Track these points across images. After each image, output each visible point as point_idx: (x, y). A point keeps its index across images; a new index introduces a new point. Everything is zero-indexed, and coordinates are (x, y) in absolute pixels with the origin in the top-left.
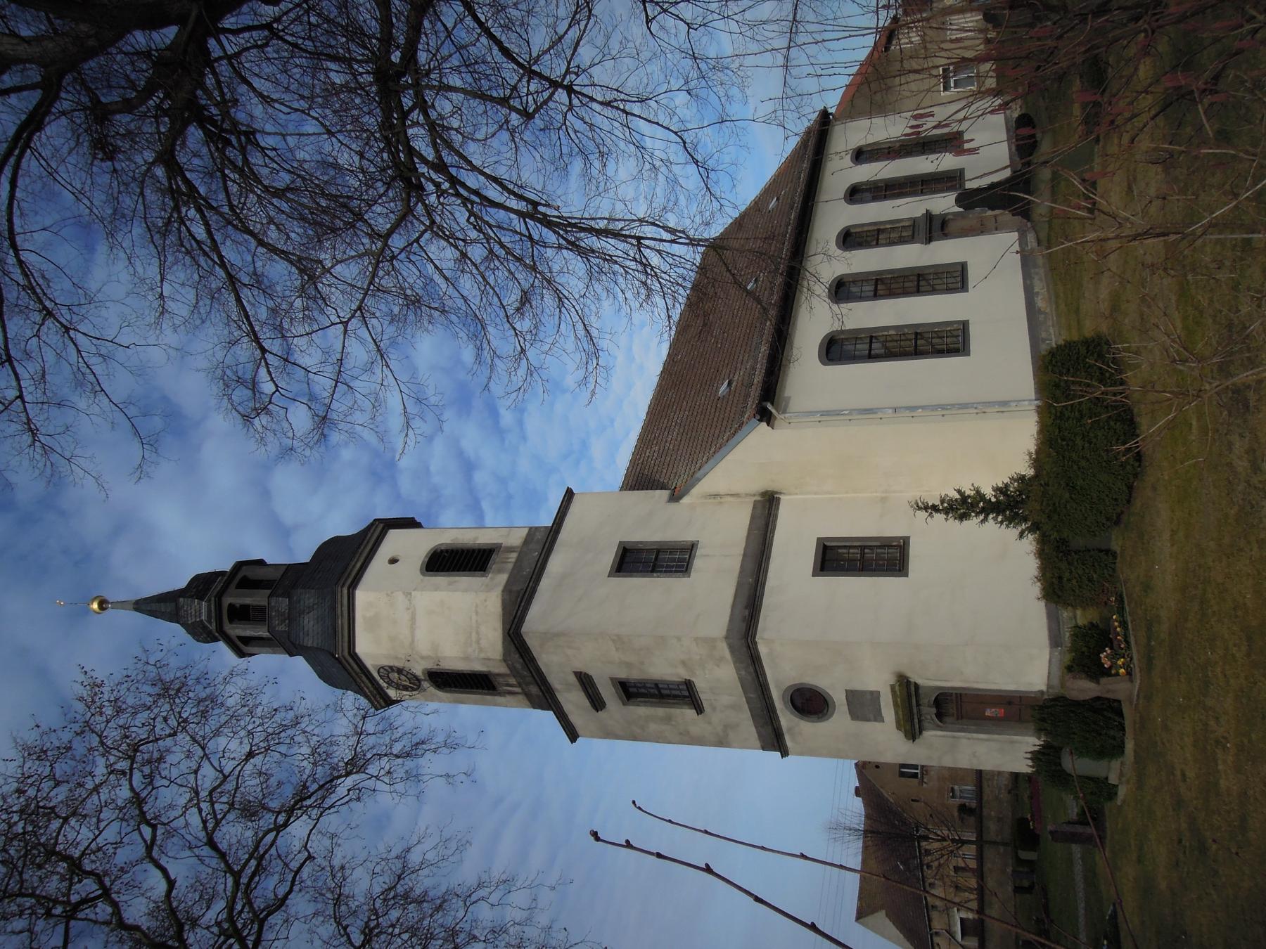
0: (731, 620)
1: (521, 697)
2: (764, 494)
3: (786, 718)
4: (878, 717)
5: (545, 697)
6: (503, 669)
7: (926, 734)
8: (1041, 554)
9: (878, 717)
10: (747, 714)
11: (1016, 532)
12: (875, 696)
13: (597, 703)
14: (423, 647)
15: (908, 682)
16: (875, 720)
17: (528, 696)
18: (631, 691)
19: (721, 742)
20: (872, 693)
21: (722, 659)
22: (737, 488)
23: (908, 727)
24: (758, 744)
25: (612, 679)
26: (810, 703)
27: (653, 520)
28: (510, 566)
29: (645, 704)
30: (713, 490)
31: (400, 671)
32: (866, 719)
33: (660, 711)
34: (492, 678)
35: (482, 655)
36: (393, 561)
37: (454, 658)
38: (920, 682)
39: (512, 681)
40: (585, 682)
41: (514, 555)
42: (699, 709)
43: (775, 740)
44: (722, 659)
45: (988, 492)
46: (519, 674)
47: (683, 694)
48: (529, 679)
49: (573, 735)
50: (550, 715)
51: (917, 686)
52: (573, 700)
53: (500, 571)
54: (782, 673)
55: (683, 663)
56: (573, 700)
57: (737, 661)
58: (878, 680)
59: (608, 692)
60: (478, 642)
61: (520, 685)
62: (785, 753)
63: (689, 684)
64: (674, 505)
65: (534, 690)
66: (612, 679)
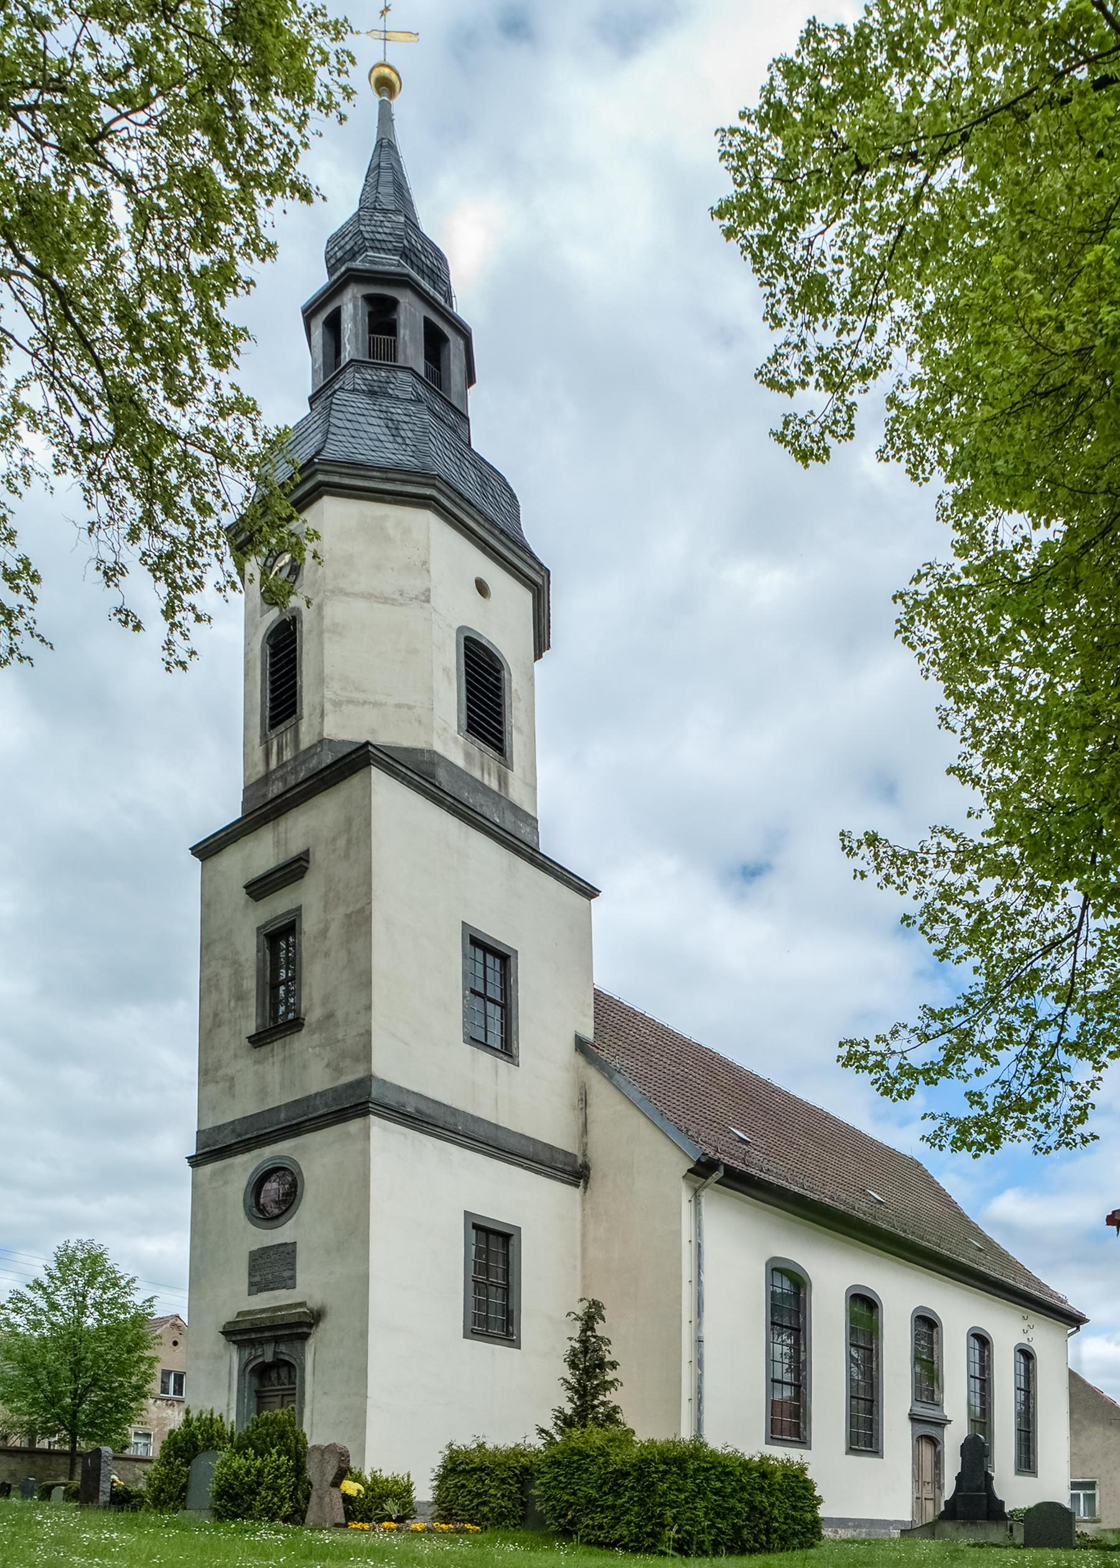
0: (400, 1089)
1: (261, 769)
2: (586, 1167)
3: (243, 1167)
4: (256, 1287)
5: (264, 809)
6: (306, 740)
7: (234, 1348)
8: (517, 1452)
9: (256, 1287)
10: (252, 1109)
11: (549, 1426)
12: (289, 1282)
13: (260, 888)
14: (335, 611)
15: (310, 1326)
16: (251, 1284)
17: (266, 779)
18: (280, 937)
19: (207, 1073)
20: (293, 1278)
21: (339, 1071)
22: (595, 1131)
23: (243, 1326)
24: (209, 1125)
25: (299, 909)
26: (275, 1196)
27: (550, 1018)
28: (477, 774)
29: (260, 962)
30: (592, 1099)
31: (295, 569)
32: (253, 1269)
33: (250, 984)
34: (292, 720)
35: (328, 707)
36: (482, 588)
37: (325, 663)
38: (311, 1341)
39: (288, 755)
40: (293, 870)
41: (494, 785)
42: (258, 1040)
43: (211, 1150)
44: (339, 1071)
45: (612, 1397)
46: (302, 772)
47: (278, 1024)
48: (292, 780)
49: (206, 851)
50: (231, 811)
51: (305, 1337)
52: (262, 853)
53: (468, 756)
54: (316, 1156)
55: (330, 1016)
56: (262, 853)
57: (336, 1093)
58: (309, 1286)
59: (279, 904)
60: (350, 702)
61: (281, 766)
62: (195, 1162)
63: (296, 1024)
64: (570, 1042)
65: (276, 789)
66: (299, 909)
